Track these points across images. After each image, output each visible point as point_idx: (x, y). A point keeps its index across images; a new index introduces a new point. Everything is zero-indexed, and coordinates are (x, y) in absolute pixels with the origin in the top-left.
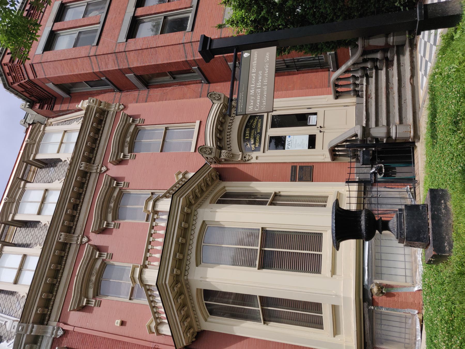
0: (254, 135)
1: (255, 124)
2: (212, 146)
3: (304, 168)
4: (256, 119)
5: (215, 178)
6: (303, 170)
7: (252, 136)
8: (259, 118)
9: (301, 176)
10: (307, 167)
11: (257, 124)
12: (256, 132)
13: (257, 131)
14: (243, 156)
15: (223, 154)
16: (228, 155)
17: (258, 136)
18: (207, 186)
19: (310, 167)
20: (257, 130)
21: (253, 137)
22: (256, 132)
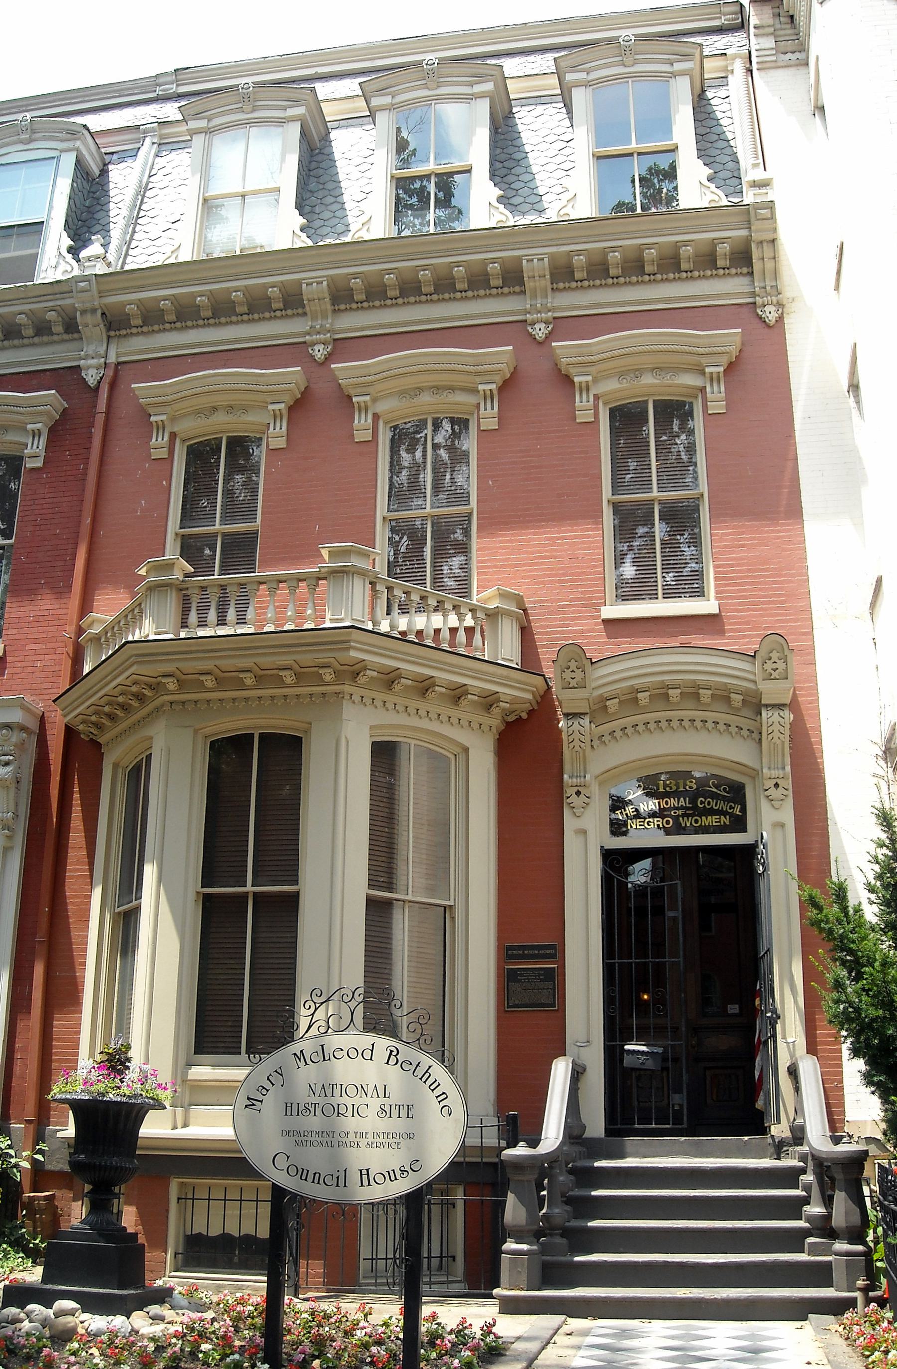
0: (670, 809)
1: (713, 803)
2: (593, 685)
3: (549, 984)
4: (731, 808)
5: (495, 710)
6: (542, 980)
7: (667, 803)
8: (731, 815)
9: (521, 975)
10: (551, 992)
11: (711, 812)
12: (680, 812)
13: (683, 816)
14: (580, 789)
15: (576, 723)
16: (576, 740)
17: (668, 822)
18: (455, 696)
19: (550, 1001)
20: (688, 816)
21: (663, 805)
22: (680, 812)
